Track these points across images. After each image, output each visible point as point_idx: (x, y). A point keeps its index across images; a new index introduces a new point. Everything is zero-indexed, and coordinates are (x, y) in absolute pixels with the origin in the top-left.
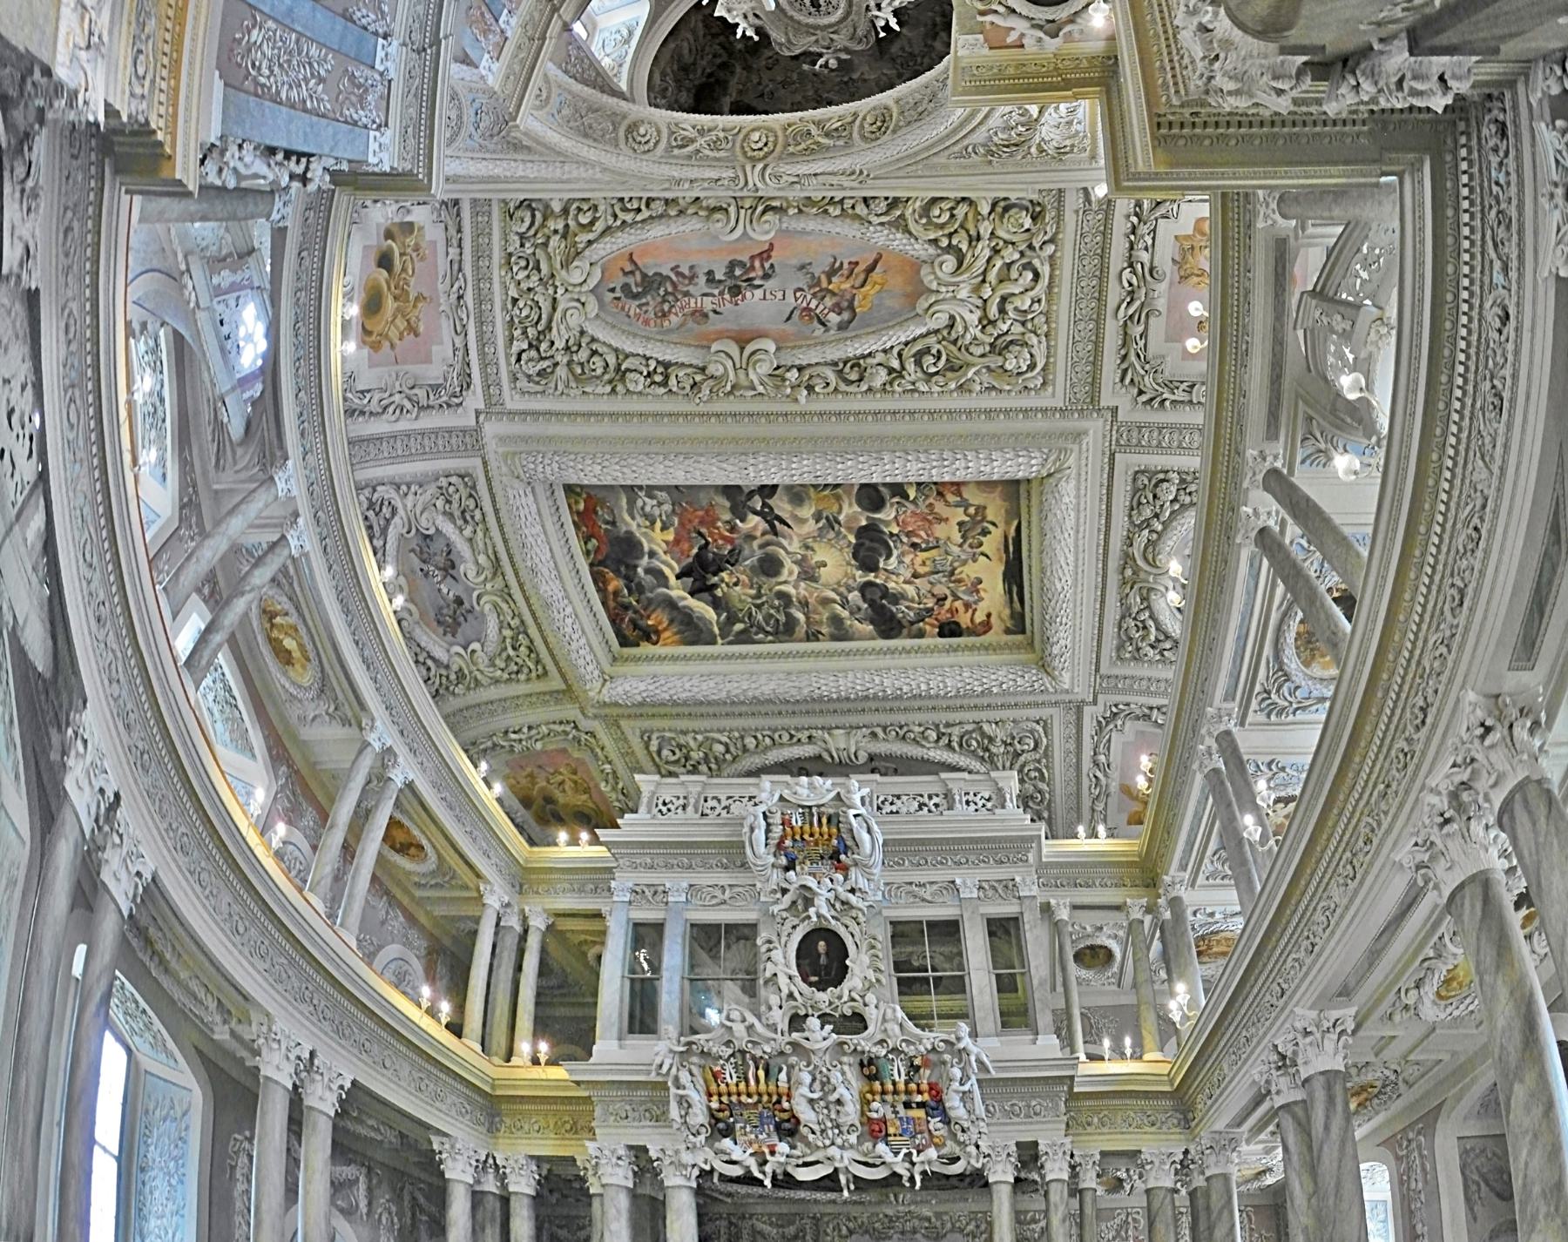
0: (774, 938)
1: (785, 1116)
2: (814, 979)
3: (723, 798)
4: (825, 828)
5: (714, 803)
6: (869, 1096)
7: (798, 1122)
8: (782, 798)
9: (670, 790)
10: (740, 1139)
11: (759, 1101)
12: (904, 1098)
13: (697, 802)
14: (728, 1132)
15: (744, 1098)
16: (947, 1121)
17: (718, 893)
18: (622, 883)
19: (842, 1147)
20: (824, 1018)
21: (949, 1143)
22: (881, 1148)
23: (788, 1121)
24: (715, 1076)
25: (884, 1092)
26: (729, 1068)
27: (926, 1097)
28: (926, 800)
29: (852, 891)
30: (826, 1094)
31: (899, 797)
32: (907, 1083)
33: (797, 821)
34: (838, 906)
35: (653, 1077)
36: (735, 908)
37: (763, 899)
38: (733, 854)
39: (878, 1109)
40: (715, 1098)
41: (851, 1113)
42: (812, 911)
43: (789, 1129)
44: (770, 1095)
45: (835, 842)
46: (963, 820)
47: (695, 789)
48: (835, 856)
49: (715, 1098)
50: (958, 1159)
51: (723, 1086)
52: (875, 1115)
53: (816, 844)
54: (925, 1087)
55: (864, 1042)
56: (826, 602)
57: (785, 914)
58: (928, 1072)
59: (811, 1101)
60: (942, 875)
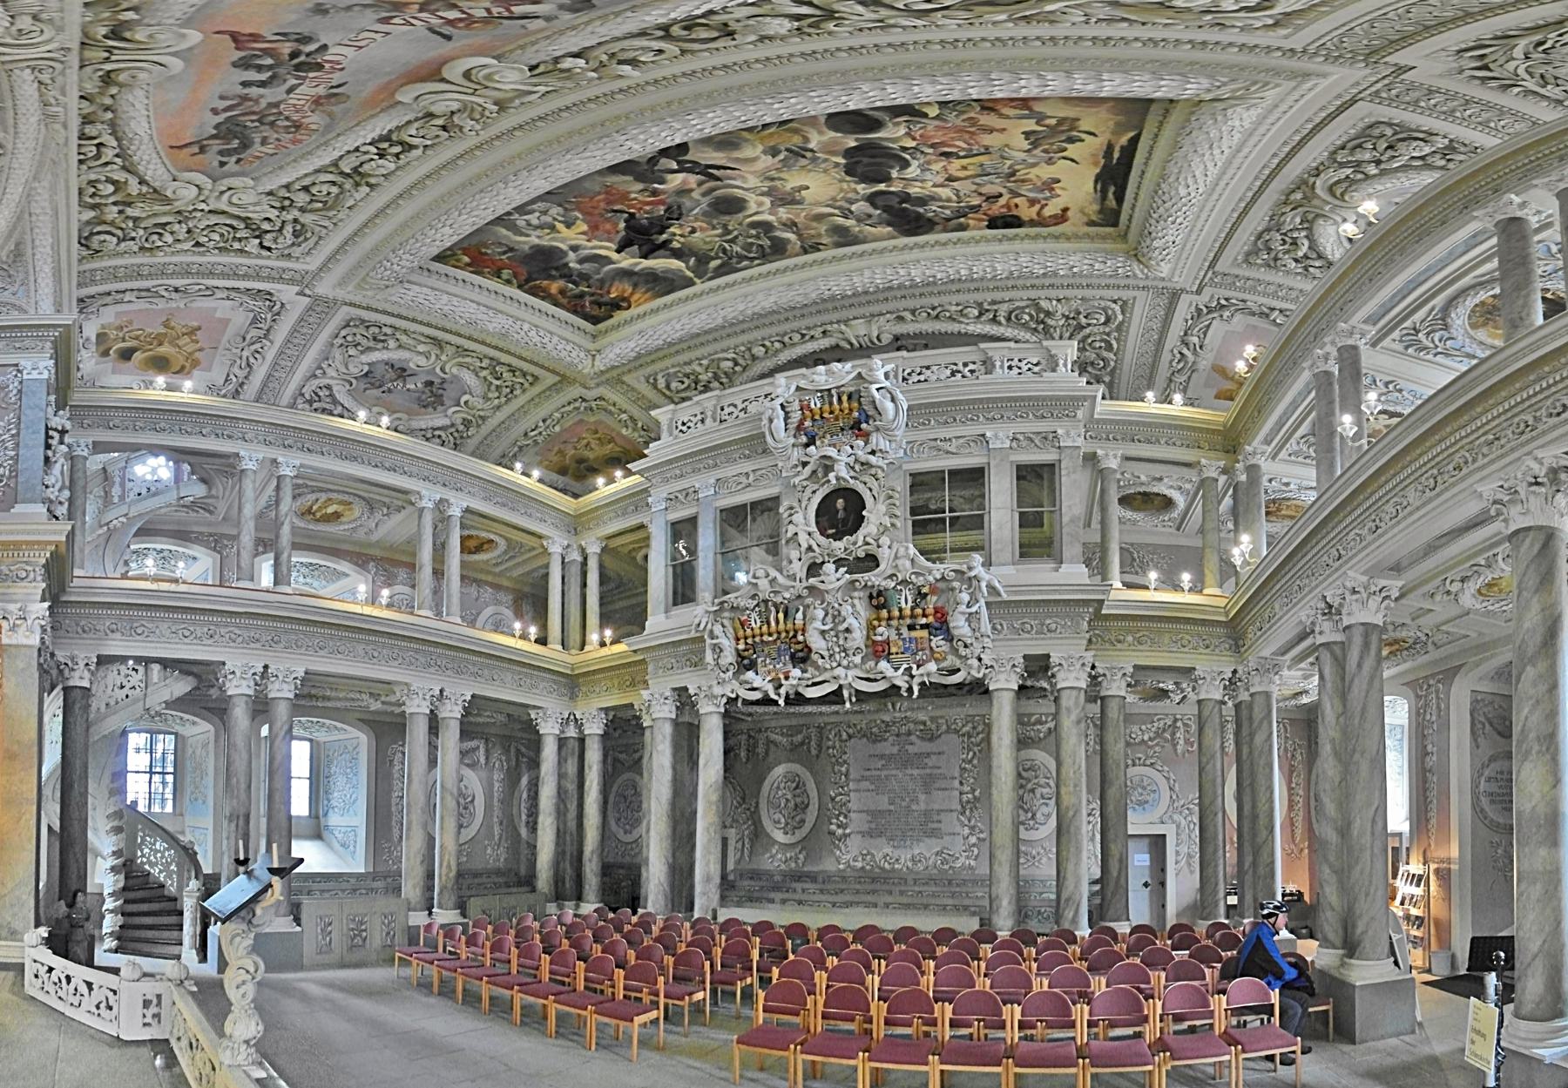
0: (795, 504)
1: (799, 647)
2: (831, 531)
4: (845, 405)
5: (732, 409)
7: (810, 650)
8: (798, 389)
10: (761, 669)
12: (908, 621)
14: (752, 666)
15: (765, 638)
16: (950, 638)
20: (839, 563)
21: (950, 657)
22: (883, 665)
24: (742, 625)
25: (890, 618)
27: (931, 619)
28: (960, 367)
29: (873, 453)
30: (836, 625)
31: (928, 368)
32: (913, 609)
33: (815, 404)
34: (857, 467)
36: (758, 488)
38: (756, 444)
39: (883, 632)
41: (858, 638)
42: (832, 476)
43: (802, 657)
45: (856, 414)
46: (1003, 381)
51: (749, 631)
53: (837, 419)
54: (930, 610)
55: (875, 578)
56: (819, 218)
59: (823, 633)
60: (972, 430)
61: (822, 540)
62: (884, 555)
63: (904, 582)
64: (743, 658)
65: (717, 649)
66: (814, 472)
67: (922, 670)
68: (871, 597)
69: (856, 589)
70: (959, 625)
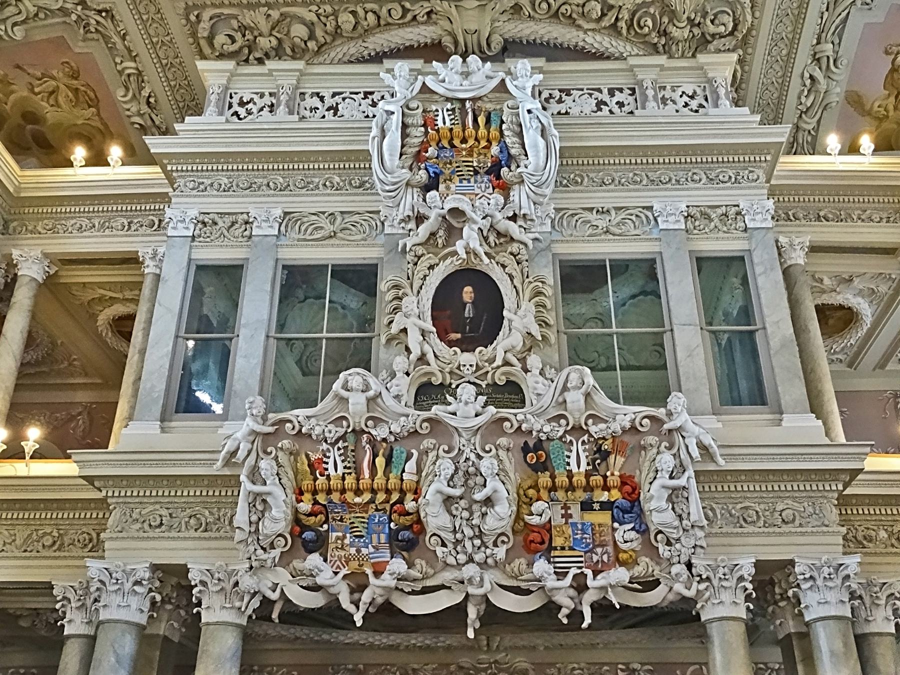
0: (406, 283)
3: (327, 94)
6: (531, 492)
7: (423, 530)
9: (251, 82)
11: (372, 501)
12: (581, 495)
13: (291, 99)
15: (349, 496)
16: (643, 530)
17: (324, 222)
18: (182, 212)
19: (483, 565)
21: (644, 560)
23: (409, 528)
25: (553, 488)
26: (335, 454)
27: (615, 495)
30: (469, 490)
32: (588, 475)
35: (216, 469)
36: (350, 243)
37: (388, 230)
39: (541, 512)
40: (307, 496)
41: (501, 516)
42: (459, 246)
43: (408, 539)
44: (388, 492)
47: (288, 82)
48: (495, 170)
49: (307, 496)
50: (657, 583)
51: (321, 480)
52: (535, 520)
54: (614, 480)
57: (420, 250)
58: (620, 460)
59: (448, 501)
61: (441, 347)
62: (532, 383)
63: (578, 430)
64: (305, 528)
65: (260, 504)
66: (433, 234)
67: (601, 580)
68: (526, 449)
69: (504, 433)
70: (659, 514)
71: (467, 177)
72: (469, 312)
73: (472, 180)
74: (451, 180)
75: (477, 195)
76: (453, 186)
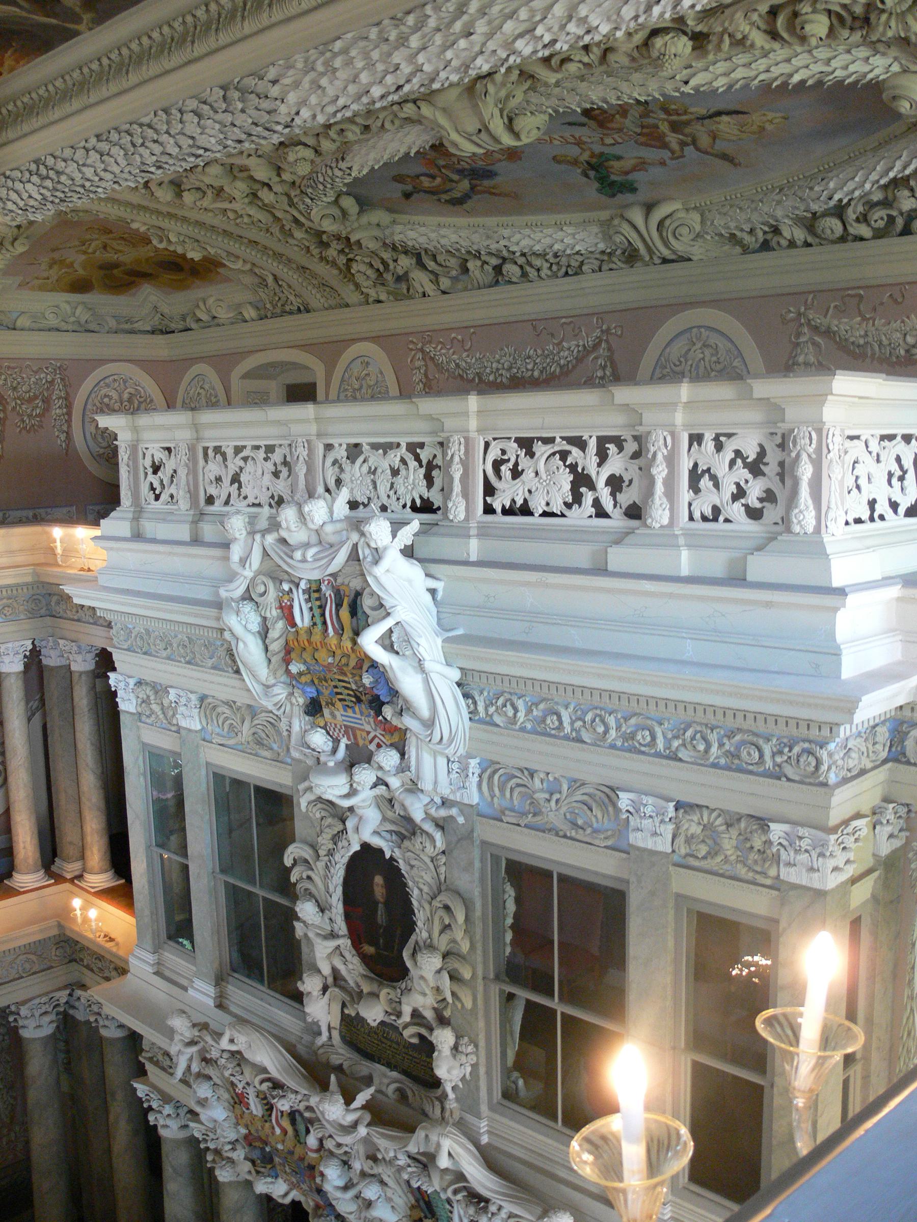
71: (351, 704)
72: (381, 916)
73: (357, 709)
74: (333, 705)
75: (368, 733)
76: (337, 713)
